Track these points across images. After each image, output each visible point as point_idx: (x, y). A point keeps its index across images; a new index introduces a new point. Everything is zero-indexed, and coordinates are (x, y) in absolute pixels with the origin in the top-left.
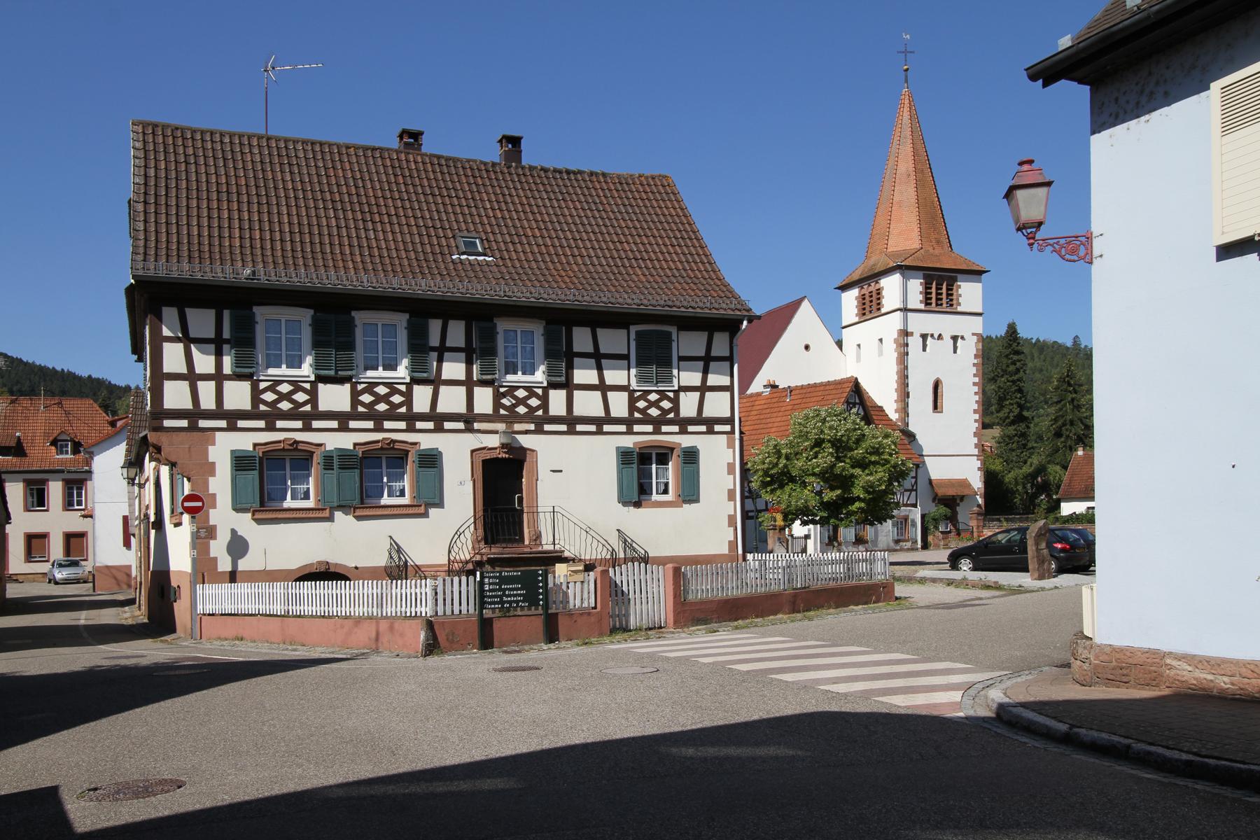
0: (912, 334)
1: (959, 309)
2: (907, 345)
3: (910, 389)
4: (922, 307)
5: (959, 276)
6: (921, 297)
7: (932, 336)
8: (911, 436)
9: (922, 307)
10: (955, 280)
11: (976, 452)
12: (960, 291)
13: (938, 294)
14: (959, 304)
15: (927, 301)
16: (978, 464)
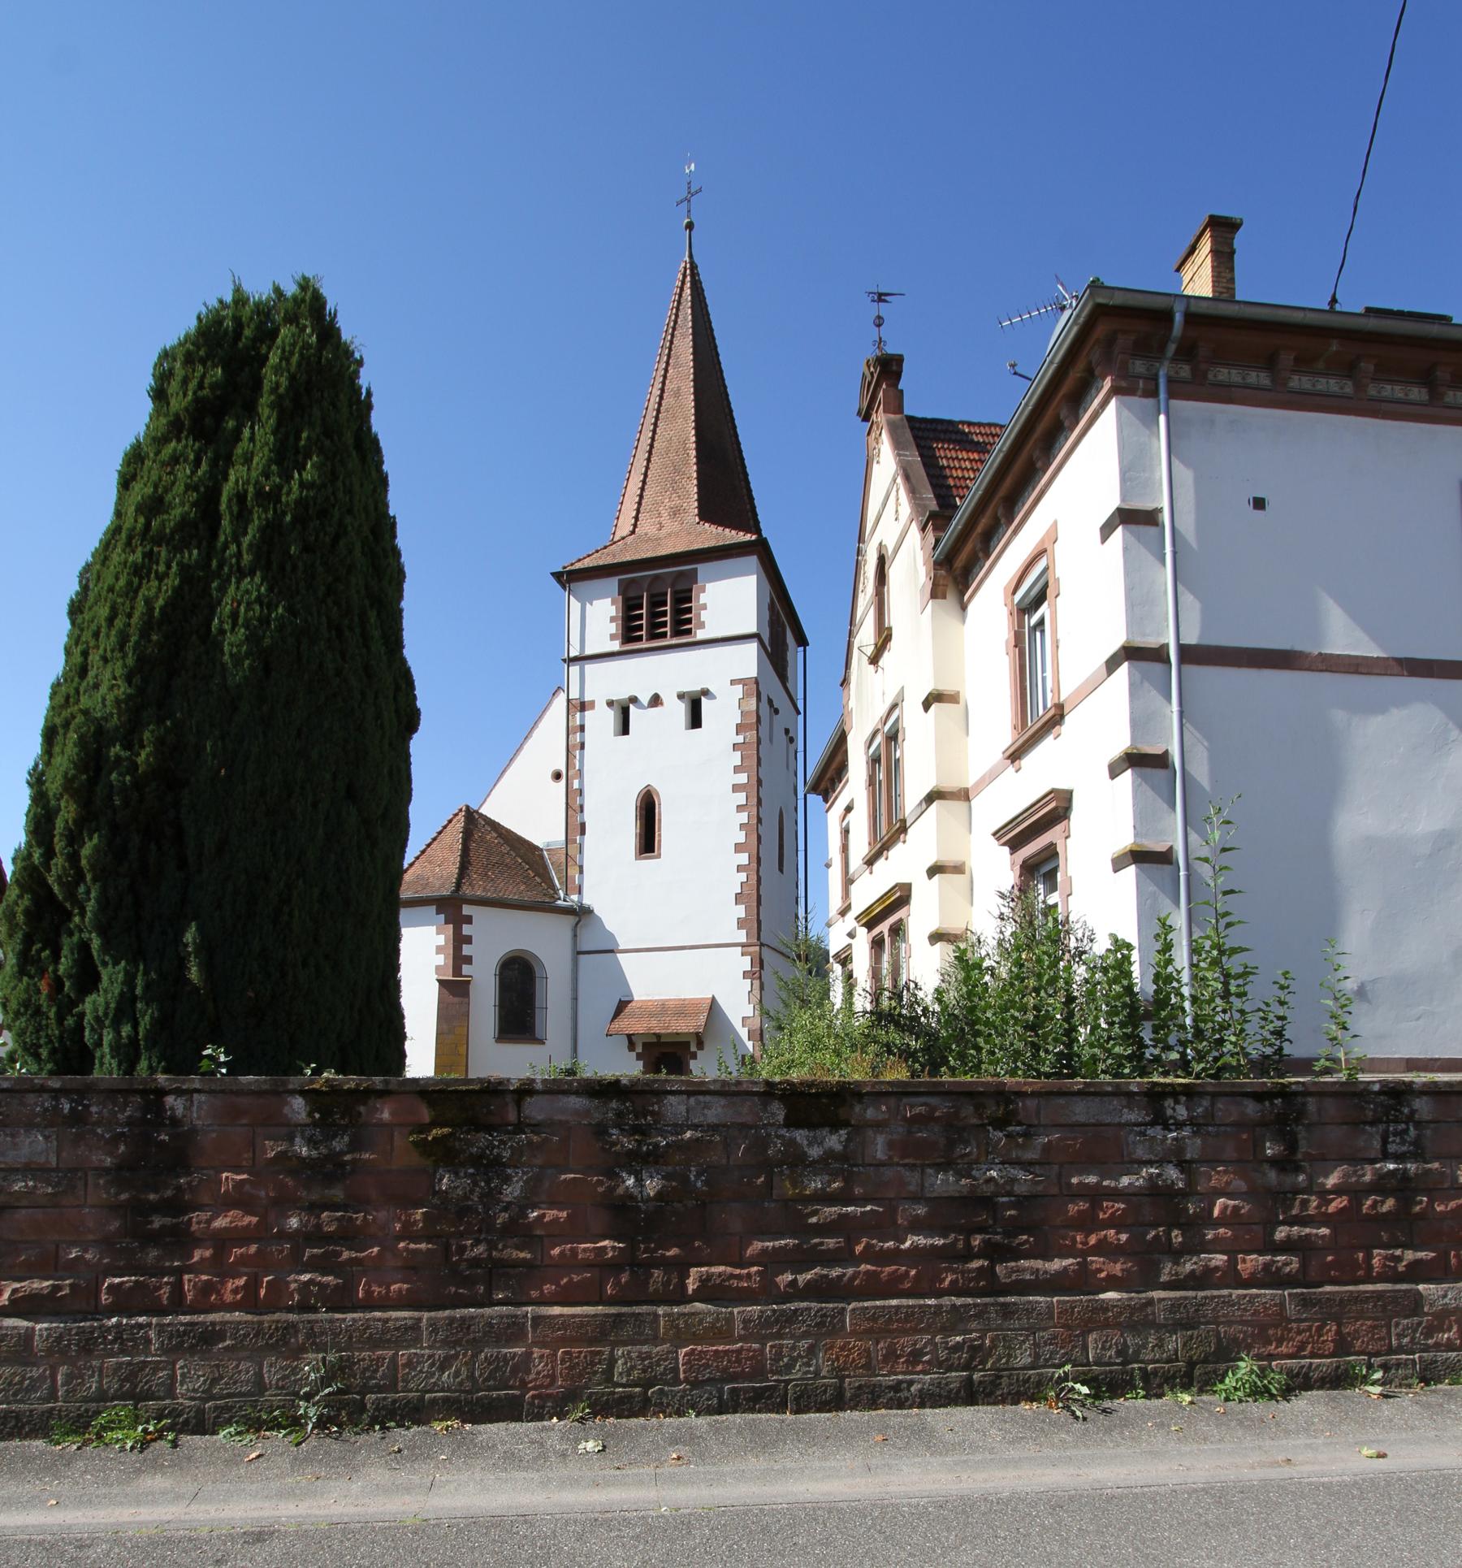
0: (592, 704)
1: (701, 635)
2: (582, 728)
3: (588, 817)
4: (616, 646)
5: (702, 569)
6: (613, 628)
7: (634, 700)
8: (582, 914)
9: (616, 646)
10: (692, 577)
11: (741, 936)
12: (703, 598)
13: (653, 615)
14: (702, 625)
15: (629, 633)
16: (746, 963)
